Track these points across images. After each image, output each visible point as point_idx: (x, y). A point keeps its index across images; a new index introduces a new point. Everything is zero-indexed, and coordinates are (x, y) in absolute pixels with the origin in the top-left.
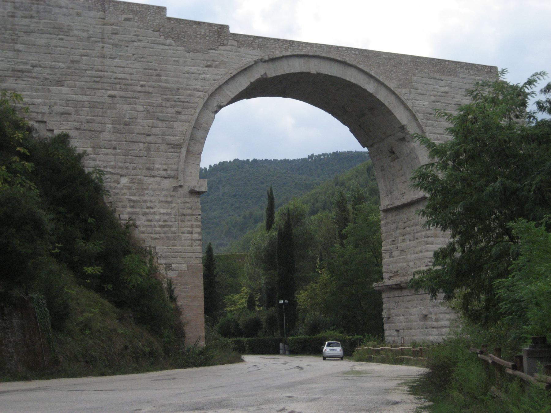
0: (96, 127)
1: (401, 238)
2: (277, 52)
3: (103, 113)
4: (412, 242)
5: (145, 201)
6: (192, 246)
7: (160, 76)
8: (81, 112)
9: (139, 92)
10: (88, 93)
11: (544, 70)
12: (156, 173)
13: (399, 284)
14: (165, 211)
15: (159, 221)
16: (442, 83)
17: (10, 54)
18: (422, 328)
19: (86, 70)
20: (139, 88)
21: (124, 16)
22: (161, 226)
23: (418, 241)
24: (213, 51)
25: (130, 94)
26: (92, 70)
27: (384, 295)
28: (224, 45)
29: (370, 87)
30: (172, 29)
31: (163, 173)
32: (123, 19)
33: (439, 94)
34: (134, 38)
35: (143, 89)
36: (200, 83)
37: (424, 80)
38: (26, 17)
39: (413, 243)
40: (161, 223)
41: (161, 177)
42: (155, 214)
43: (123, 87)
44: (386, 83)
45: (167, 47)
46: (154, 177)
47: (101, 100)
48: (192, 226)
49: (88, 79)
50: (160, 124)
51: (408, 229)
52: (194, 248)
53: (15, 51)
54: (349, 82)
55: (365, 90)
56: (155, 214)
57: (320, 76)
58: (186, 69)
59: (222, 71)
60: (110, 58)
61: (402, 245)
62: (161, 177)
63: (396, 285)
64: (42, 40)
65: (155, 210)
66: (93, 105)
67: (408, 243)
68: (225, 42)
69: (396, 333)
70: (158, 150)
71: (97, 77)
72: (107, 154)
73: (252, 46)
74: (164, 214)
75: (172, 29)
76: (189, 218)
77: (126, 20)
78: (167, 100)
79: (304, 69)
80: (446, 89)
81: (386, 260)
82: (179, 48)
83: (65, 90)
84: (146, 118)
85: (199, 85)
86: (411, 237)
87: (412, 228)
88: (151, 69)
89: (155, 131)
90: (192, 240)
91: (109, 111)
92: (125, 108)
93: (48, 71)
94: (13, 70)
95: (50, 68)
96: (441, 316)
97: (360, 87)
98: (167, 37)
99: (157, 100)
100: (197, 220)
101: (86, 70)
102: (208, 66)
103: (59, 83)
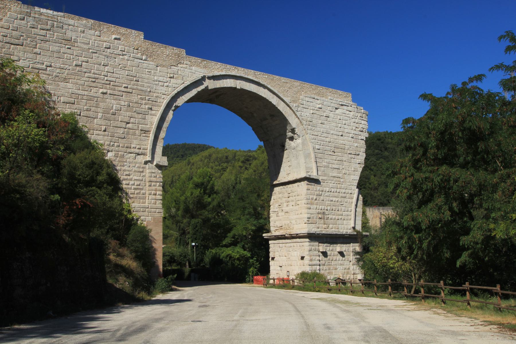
0: (91, 114)
1: (285, 204)
2: (216, 72)
3: (97, 105)
4: (294, 207)
5: (124, 170)
6: (156, 204)
7: (138, 81)
8: (81, 103)
9: (123, 92)
10: (86, 89)
11: (421, 100)
12: (132, 150)
13: (284, 235)
14: (138, 178)
15: (134, 184)
16: (319, 102)
17: (31, 56)
18: (300, 265)
19: (85, 72)
20: (123, 89)
21: (114, 37)
22: (135, 189)
23: (299, 206)
24: (174, 67)
25: (116, 93)
26: (90, 72)
27: (270, 242)
28: (180, 63)
29: (274, 100)
30: (147, 49)
31: (137, 151)
32: (113, 38)
33: (316, 109)
34: (120, 53)
35: (125, 90)
36: (164, 89)
37: (307, 99)
38: (43, 30)
39: (295, 208)
40: (135, 187)
41: (136, 153)
42: (131, 180)
43: (111, 87)
44: (284, 98)
45: (143, 61)
46: (131, 153)
47: (96, 95)
48: (156, 190)
49: (87, 79)
50: (136, 115)
51: (291, 198)
52: (157, 205)
53: (35, 53)
54: (261, 96)
55: (270, 103)
56: (131, 180)
57: (242, 90)
58: (156, 78)
59: (180, 81)
60: (103, 65)
61: (285, 209)
62: (136, 153)
63: (282, 235)
64: (54, 47)
65: (131, 177)
66: (90, 99)
67: (292, 207)
68: (182, 62)
69: (279, 268)
70: (134, 134)
71: (94, 78)
72: (98, 135)
73: (200, 66)
74: (136, 180)
75: (147, 49)
76: (154, 183)
77: (115, 39)
78: (142, 99)
79: (233, 85)
80: (320, 106)
81: (273, 218)
82: (151, 63)
83: (69, 85)
84: (127, 111)
85: (163, 90)
86: (293, 203)
87: (295, 198)
88: (131, 76)
89: (132, 120)
90: (156, 199)
91: (101, 104)
92: (114, 104)
93: (58, 71)
94: (32, 68)
95: (59, 68)
96: (314, 258)
97: (268, 100)
98: (143, 54)
99: (135, 98)
100: (159, 186)
101: (85, 72)
102: (170, 78)
103: (66, 80)
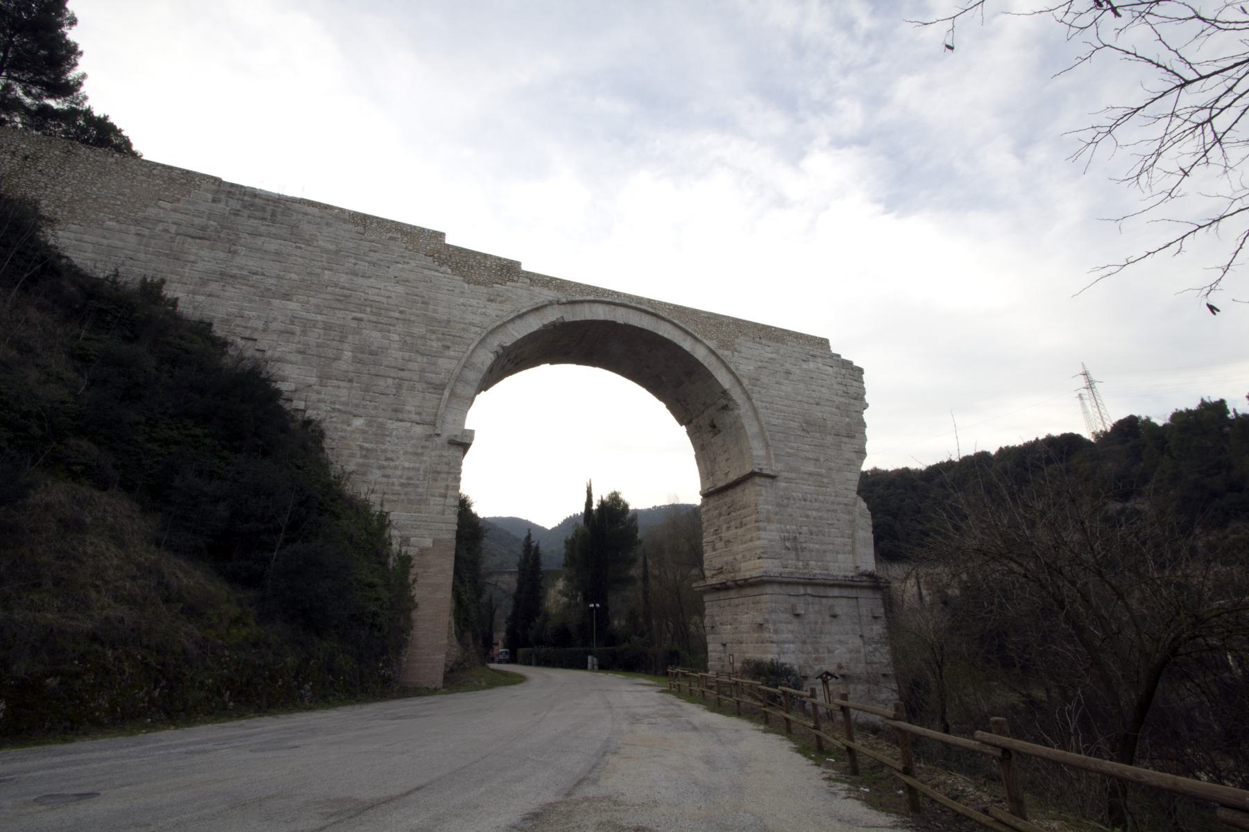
1: (724, 527)
5: (385, 451)
12: (406, 416)
15: (401, 477)
17: (222, 255)
20: (397, 315)
22: (402, 485)
25: (384, 320)
27: (706, 598)
28: (513, 281)
29: (687, 345)
31: (416, 418)
39: (740, 531)
40: (403, 481)
42: (396, 468)
46: (401, 421)
49: (328, 297)
50: (419, 358)
54: (662, 337)
55: (680, 348)
56: (396, 468)
61: (725, 535)
66: (328, 327)
69: (721, 648)
70: (412, 389)
72: (339, 387)
77: (391, 238)
79: (609, 318)
80: (774, 356)
81: (708, 554)
83: (292, 305)
84: (400, 349)
85: (477, 319)
89: (411, 365)
93: (273, 281)
97: (675, 345)
99: (420, 330)
103: (286, 297)
